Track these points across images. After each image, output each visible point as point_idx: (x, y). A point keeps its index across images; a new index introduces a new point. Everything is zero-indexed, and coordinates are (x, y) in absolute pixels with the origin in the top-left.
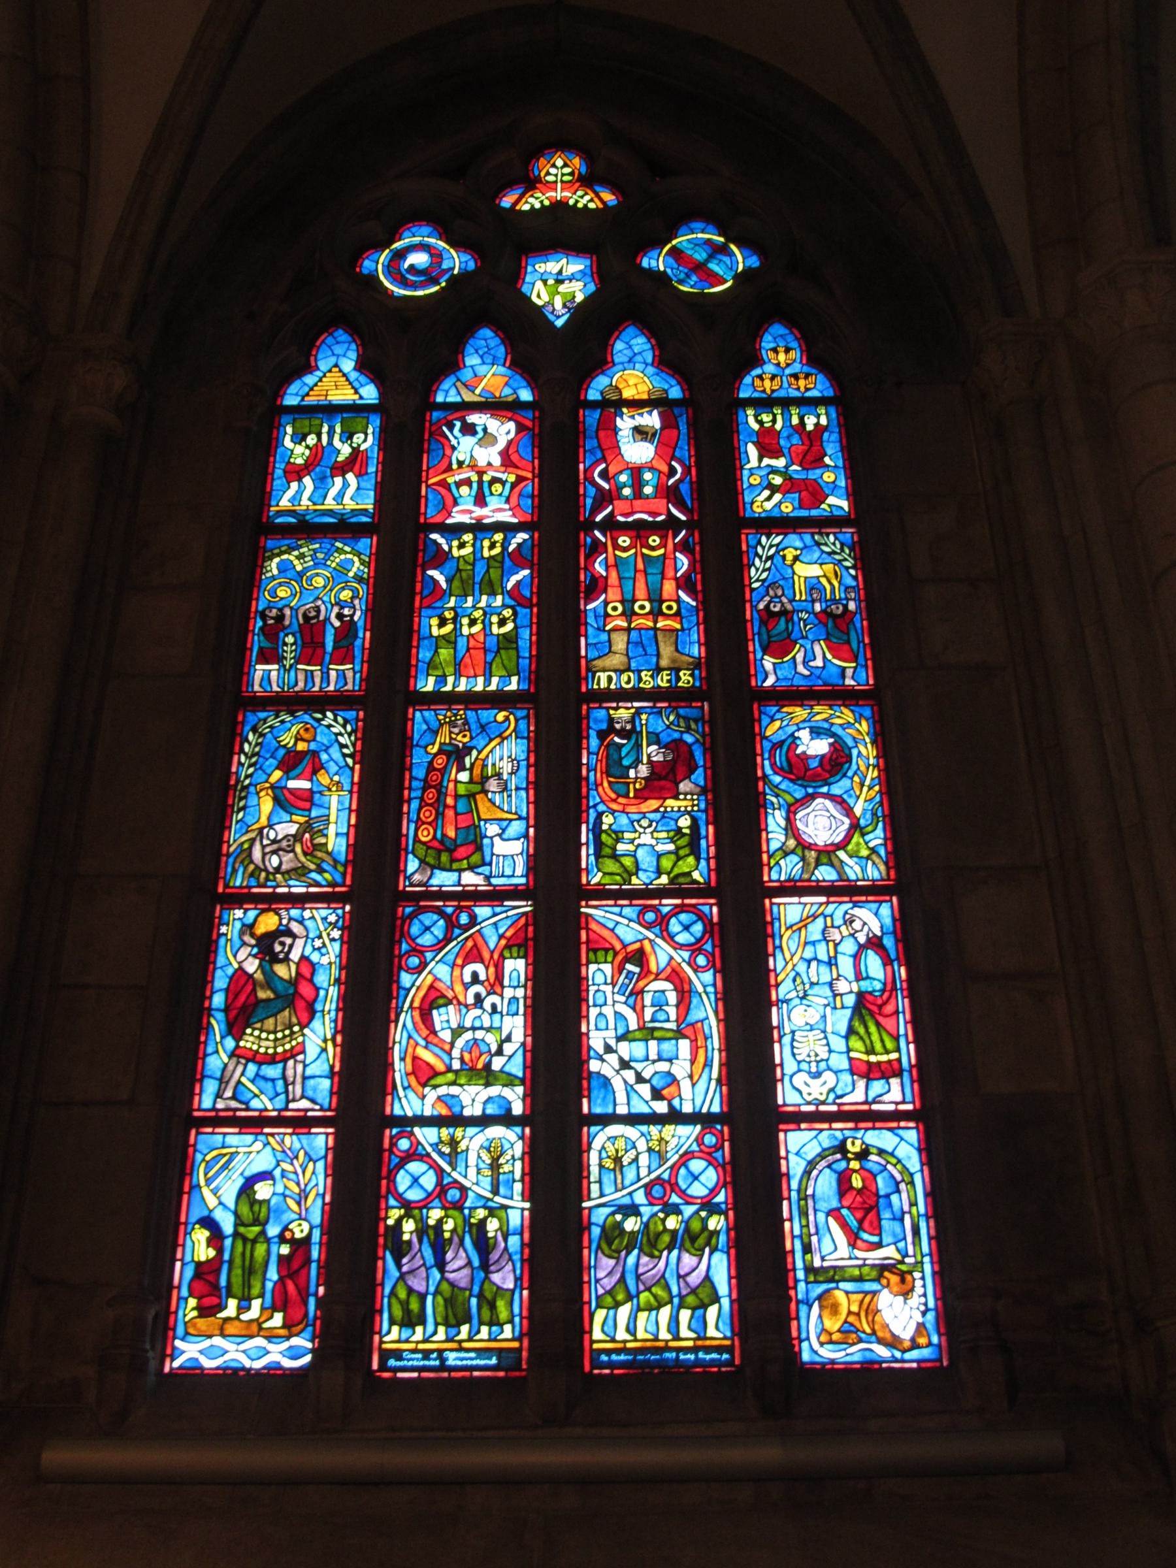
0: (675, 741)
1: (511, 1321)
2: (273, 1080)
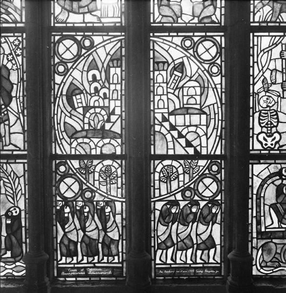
1: (118, 255)
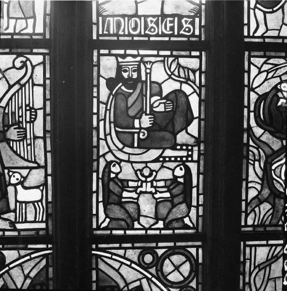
0: (175, 92)
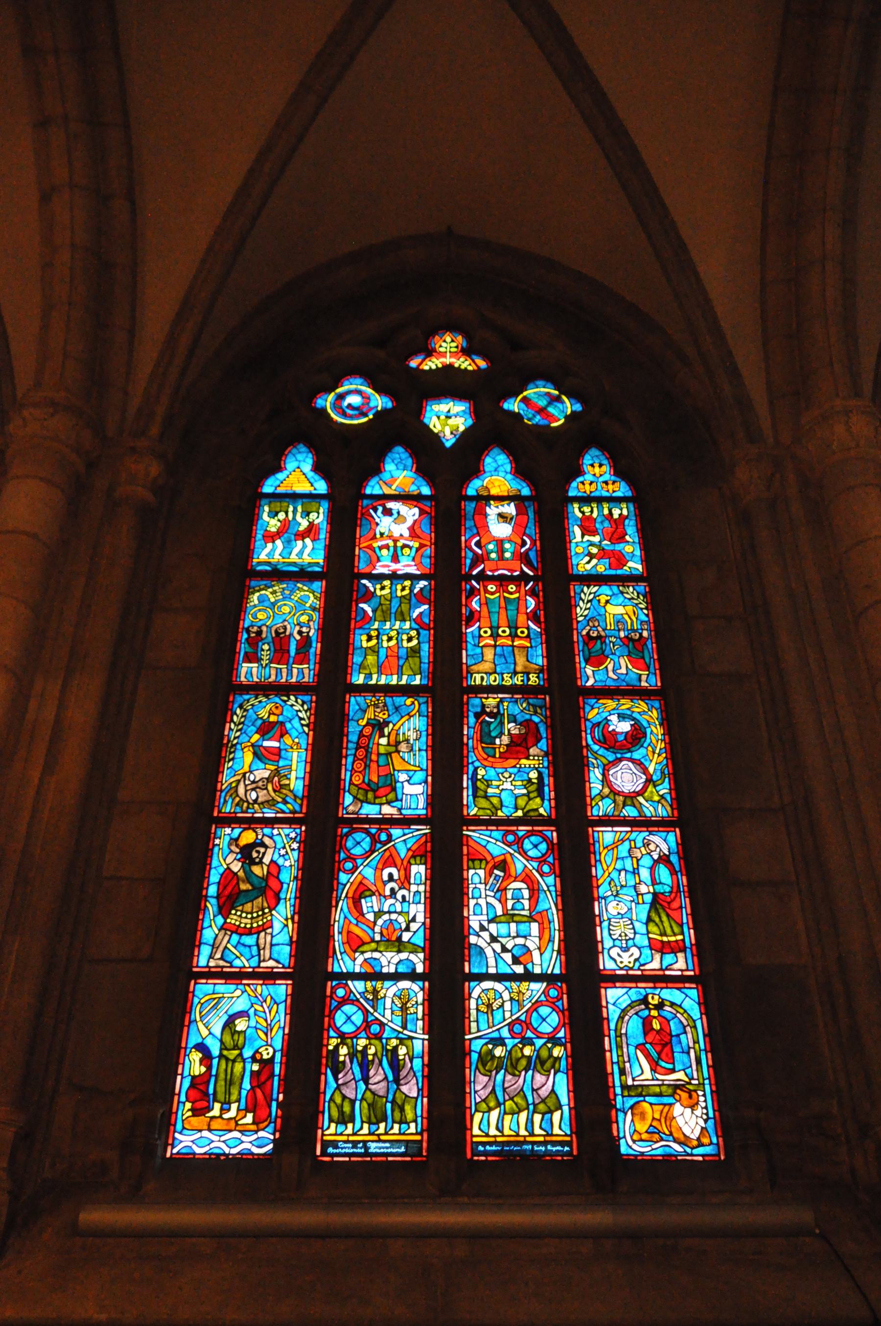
0: (526, 721)
1: (415, 1121)
2: (250, 947)
